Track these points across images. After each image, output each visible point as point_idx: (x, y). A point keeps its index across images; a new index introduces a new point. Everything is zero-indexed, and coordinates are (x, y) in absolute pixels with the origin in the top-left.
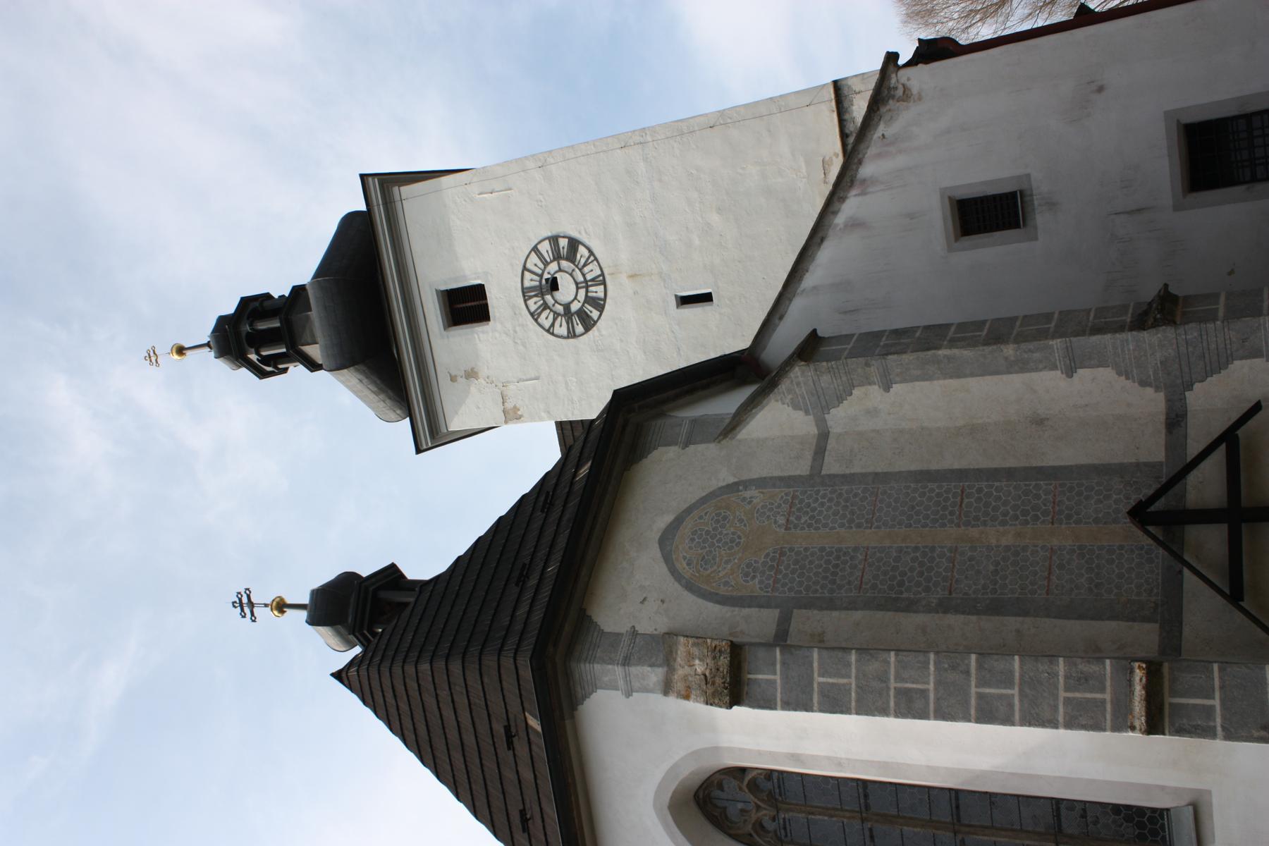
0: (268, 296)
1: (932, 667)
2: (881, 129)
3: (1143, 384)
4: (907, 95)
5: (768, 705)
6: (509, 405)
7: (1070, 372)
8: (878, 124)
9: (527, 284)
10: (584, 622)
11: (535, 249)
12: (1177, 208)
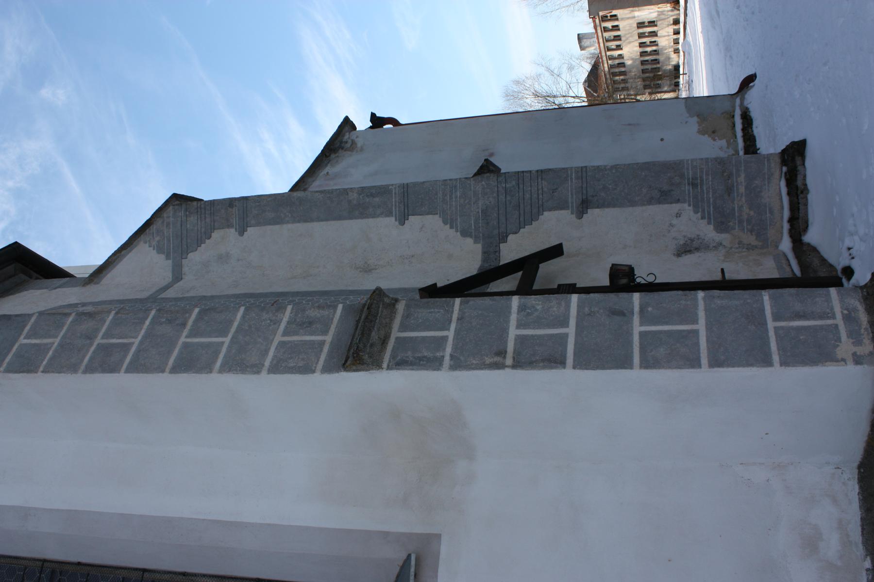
1: (147, 322)
2: (329, 169)
3: (465, 234)
8: (326, 165)
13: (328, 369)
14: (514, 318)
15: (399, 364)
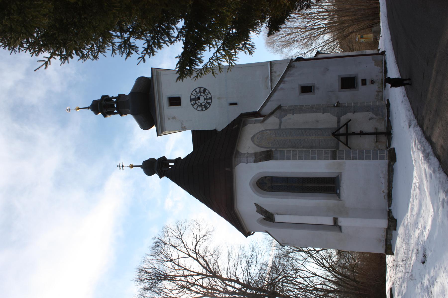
0: (108, 96)
2: (289, 72)
4: (294, 67)
5: (277, 159)
6: (183, 126)
7: (323, 113)
9: (192, 98)
10: (238, 152)
11: (195, 90)
12: (339, 91)
13: (331, 160)
14: (351, 153)
15: (339, 159)
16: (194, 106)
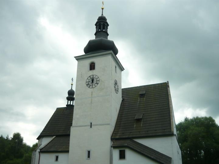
11: (98, 78)
16: (89, 78)
